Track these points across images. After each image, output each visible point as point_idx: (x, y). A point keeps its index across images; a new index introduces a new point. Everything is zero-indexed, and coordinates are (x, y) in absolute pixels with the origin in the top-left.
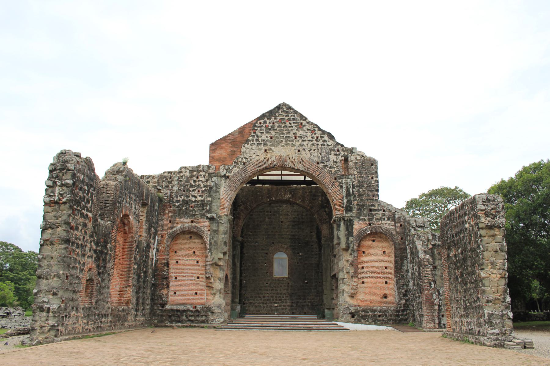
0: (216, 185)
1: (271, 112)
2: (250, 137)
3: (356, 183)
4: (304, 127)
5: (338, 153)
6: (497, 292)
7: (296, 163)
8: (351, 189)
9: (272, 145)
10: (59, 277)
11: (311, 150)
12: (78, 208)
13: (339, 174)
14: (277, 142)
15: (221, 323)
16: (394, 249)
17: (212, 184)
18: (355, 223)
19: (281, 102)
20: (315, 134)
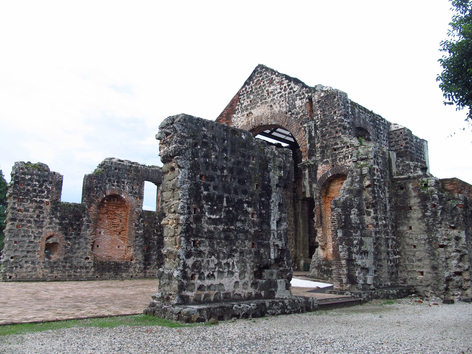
3: (319, 123)
4: (274, 81)
6: (174, 243)
8: (313, 131)
12: (26, 197)
18: (318, 168)
19: (257, 65)
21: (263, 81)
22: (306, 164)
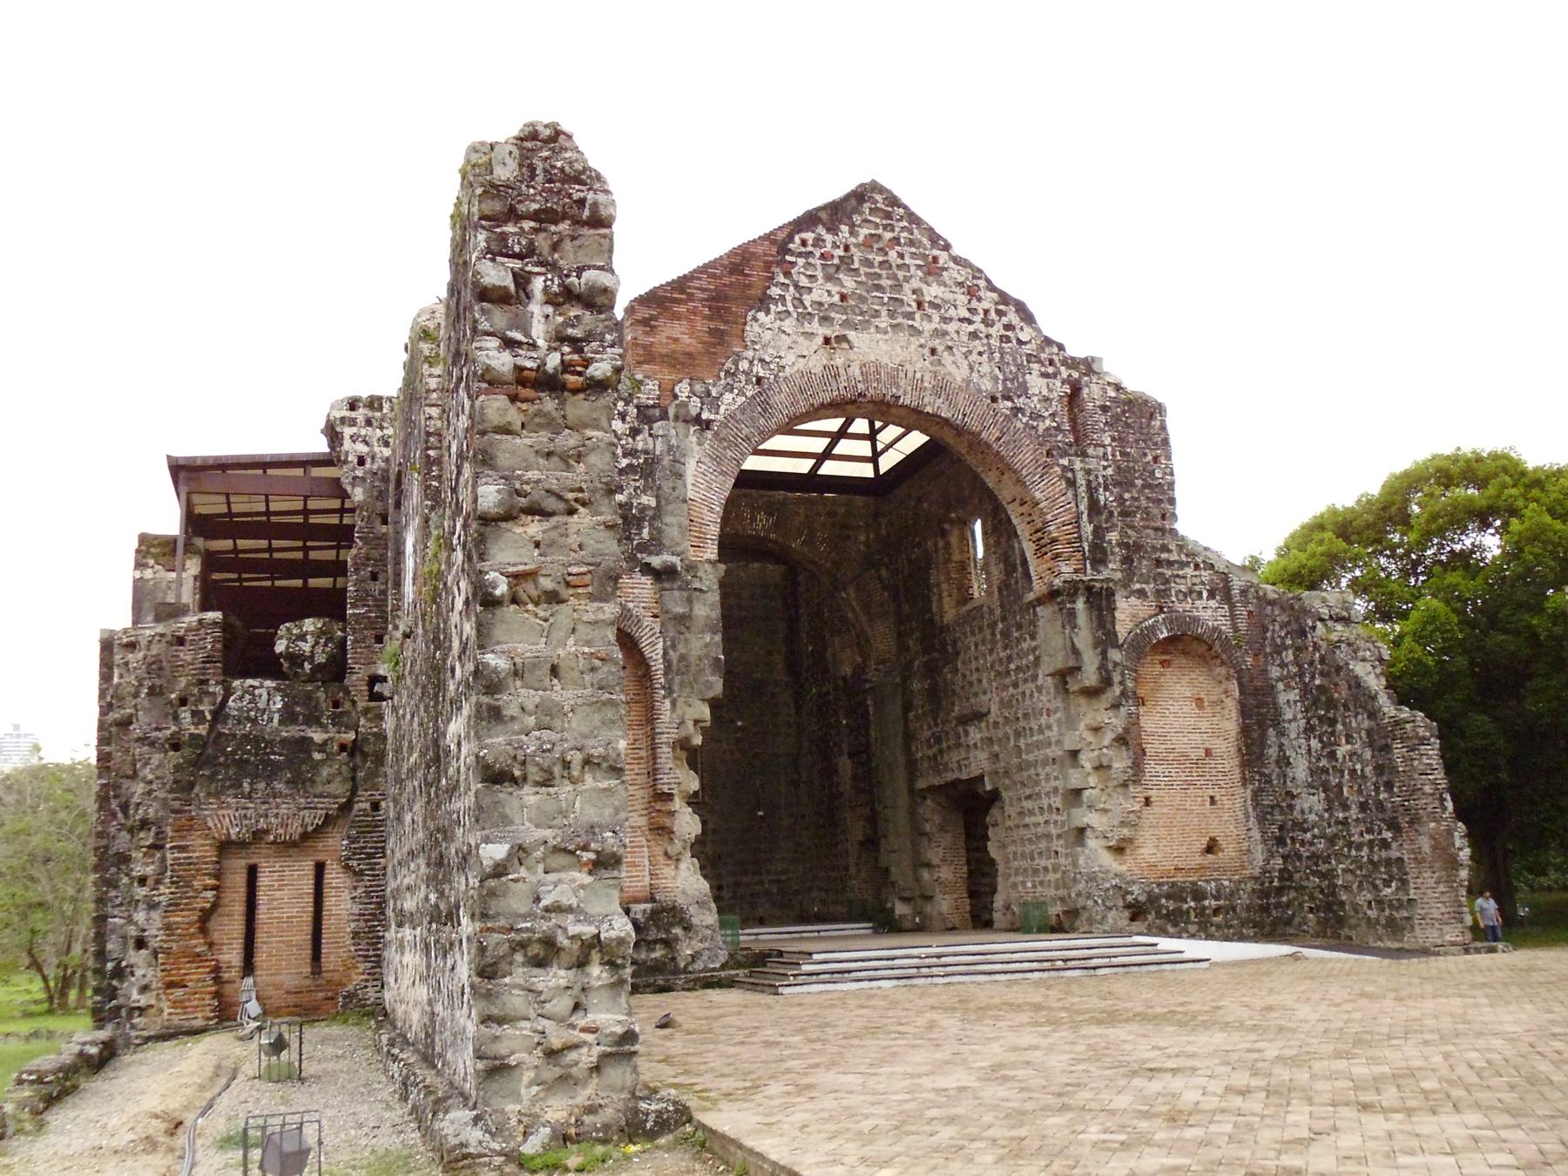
0: (670, 448)
1: (836, 208)
2: (773, 288)
3: (1110, 471)
4: (945, 273)
5: (1051, 370)
7: (928, 393)
9: (846, 324)
10: (616, 771)
11: (970, 352)
13: (1059, 438)
14: (862, 313)
15: (723, 967)
16: (1237, 694)
17: (660, 447)
18: (1118, 604)
19: (867, 180)
20: (979, 299)
21: (898, 248)
22: (1098, 585)
